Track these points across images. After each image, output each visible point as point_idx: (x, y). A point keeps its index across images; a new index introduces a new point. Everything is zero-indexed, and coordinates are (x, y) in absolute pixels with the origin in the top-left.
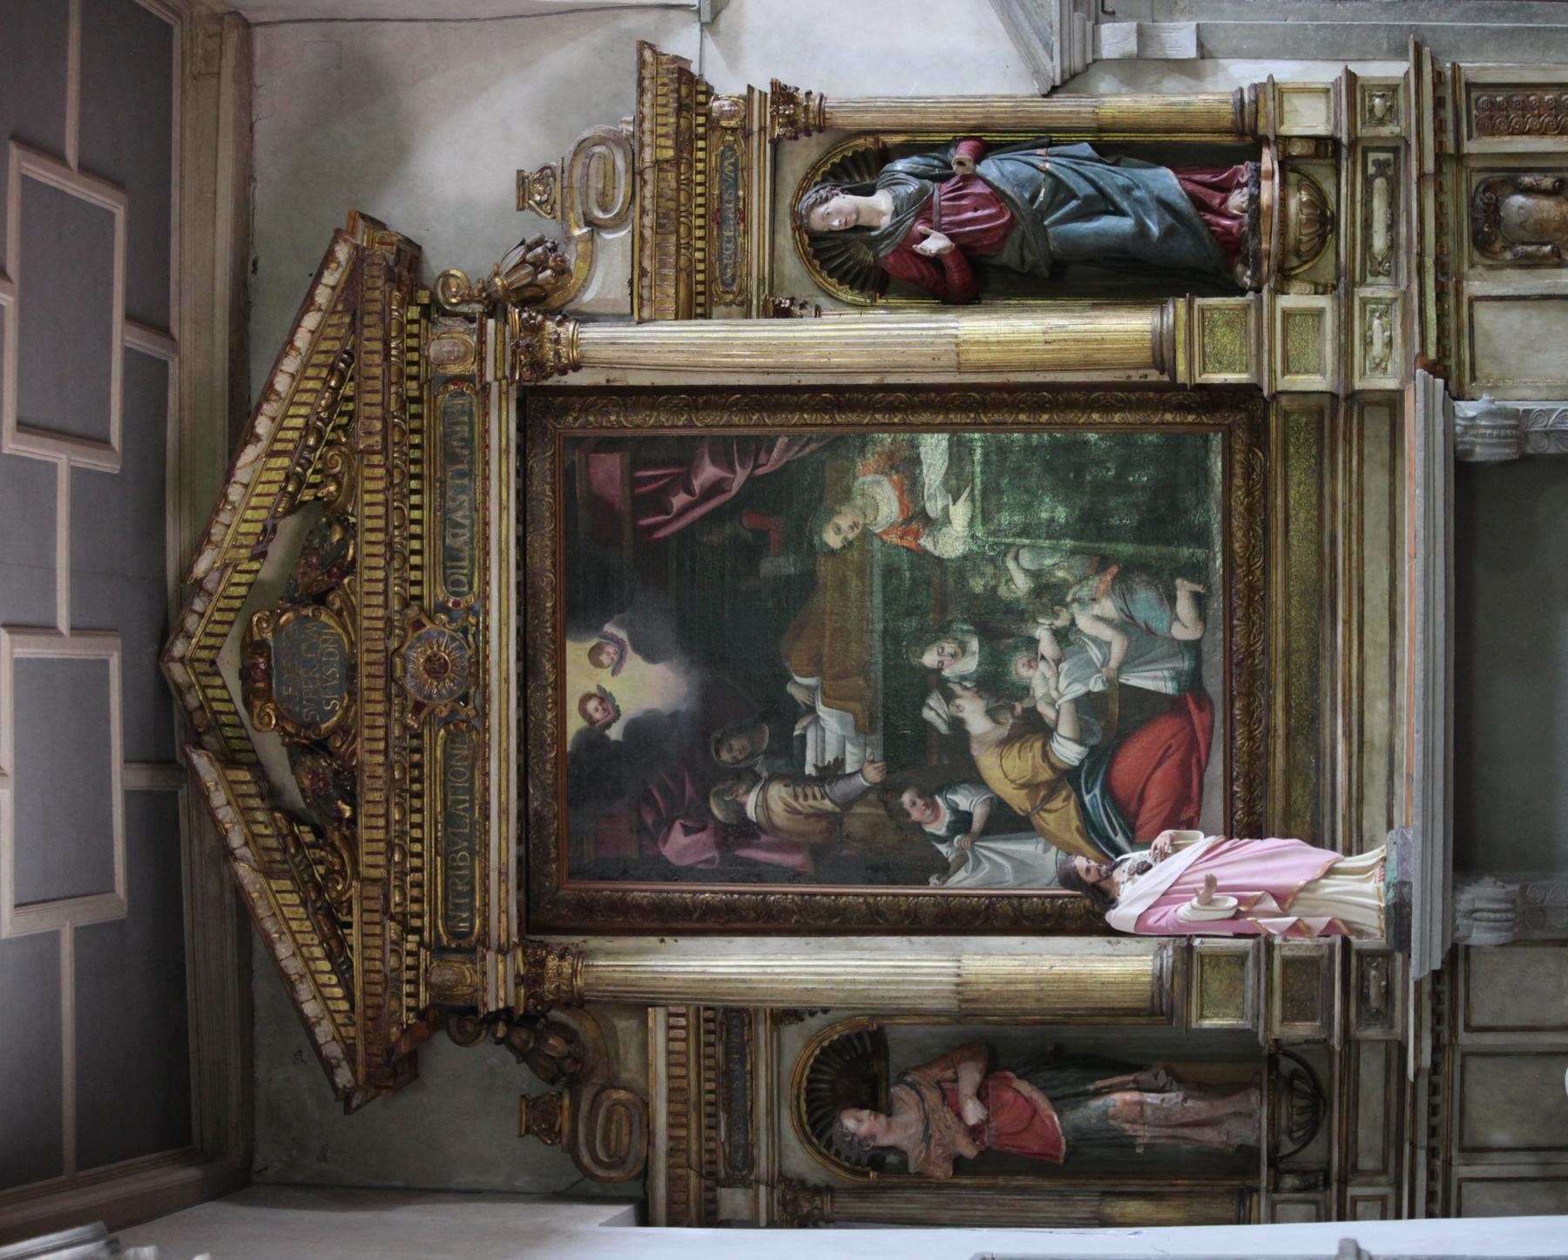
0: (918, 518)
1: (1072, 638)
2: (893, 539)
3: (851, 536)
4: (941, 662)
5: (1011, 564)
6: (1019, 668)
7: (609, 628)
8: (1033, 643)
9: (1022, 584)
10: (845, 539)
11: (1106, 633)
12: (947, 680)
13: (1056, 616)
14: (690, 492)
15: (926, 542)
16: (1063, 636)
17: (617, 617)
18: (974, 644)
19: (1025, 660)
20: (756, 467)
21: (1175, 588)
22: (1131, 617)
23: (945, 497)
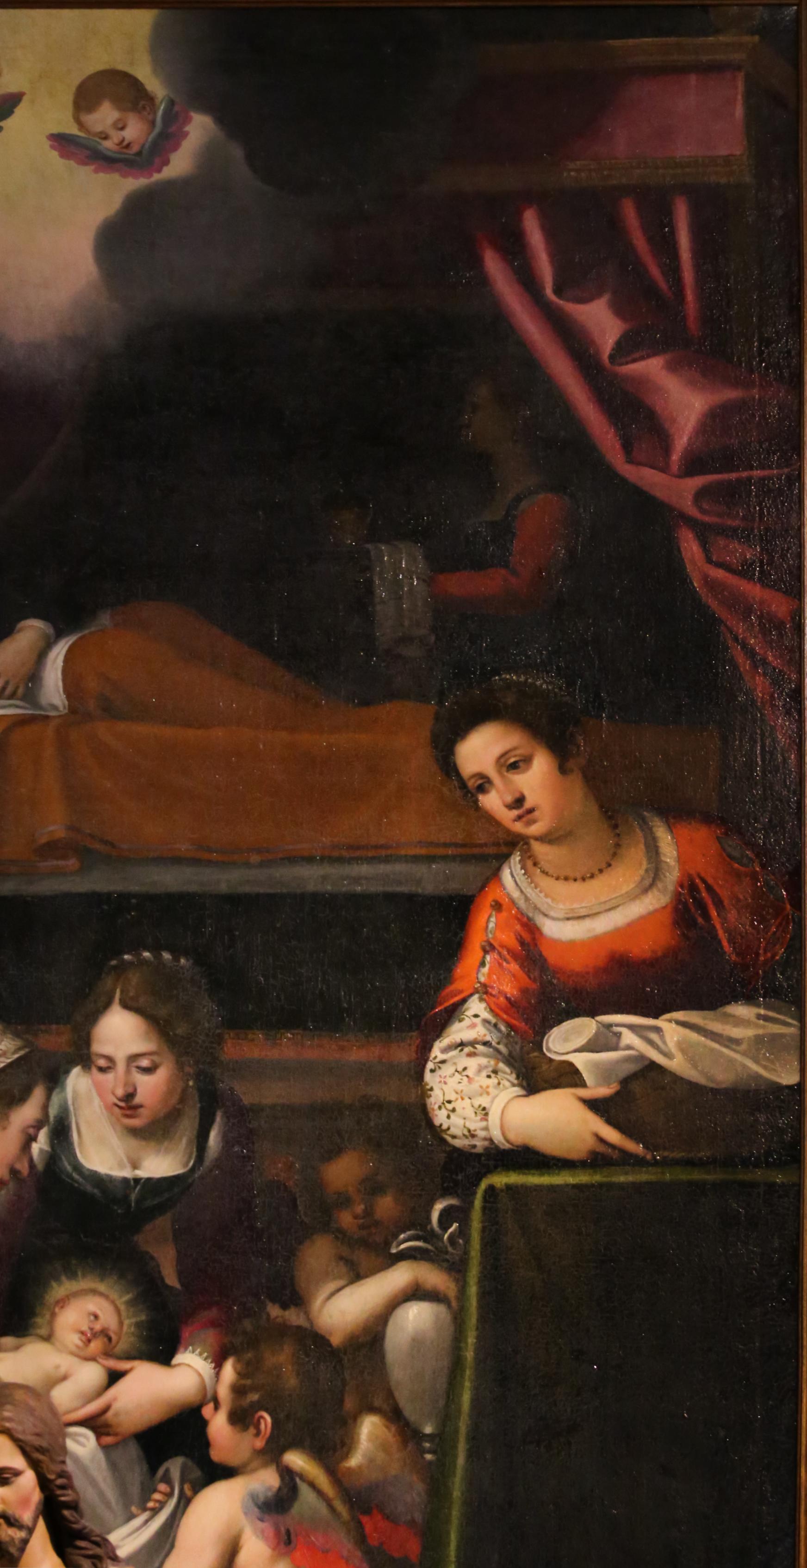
0: (549, 994)
1: (175, 1466)
2: (487, 925)
3: (493, 802)
4: (110, 1065)
5: (399, 1277)
6: (86, 1308)
7: (200, 128)
8: (161, 1349)
9: (343, 1308)
10: (484, 784)
12: (54, 1079)
13: (240, 1418)
14: (626, 348)
15: (474, 1022)
16: (173, 1447)
17: (237, 152)
18: (161, 1164)
19: (108, 1318)
20: (704, 533)
23: (604, 1073)
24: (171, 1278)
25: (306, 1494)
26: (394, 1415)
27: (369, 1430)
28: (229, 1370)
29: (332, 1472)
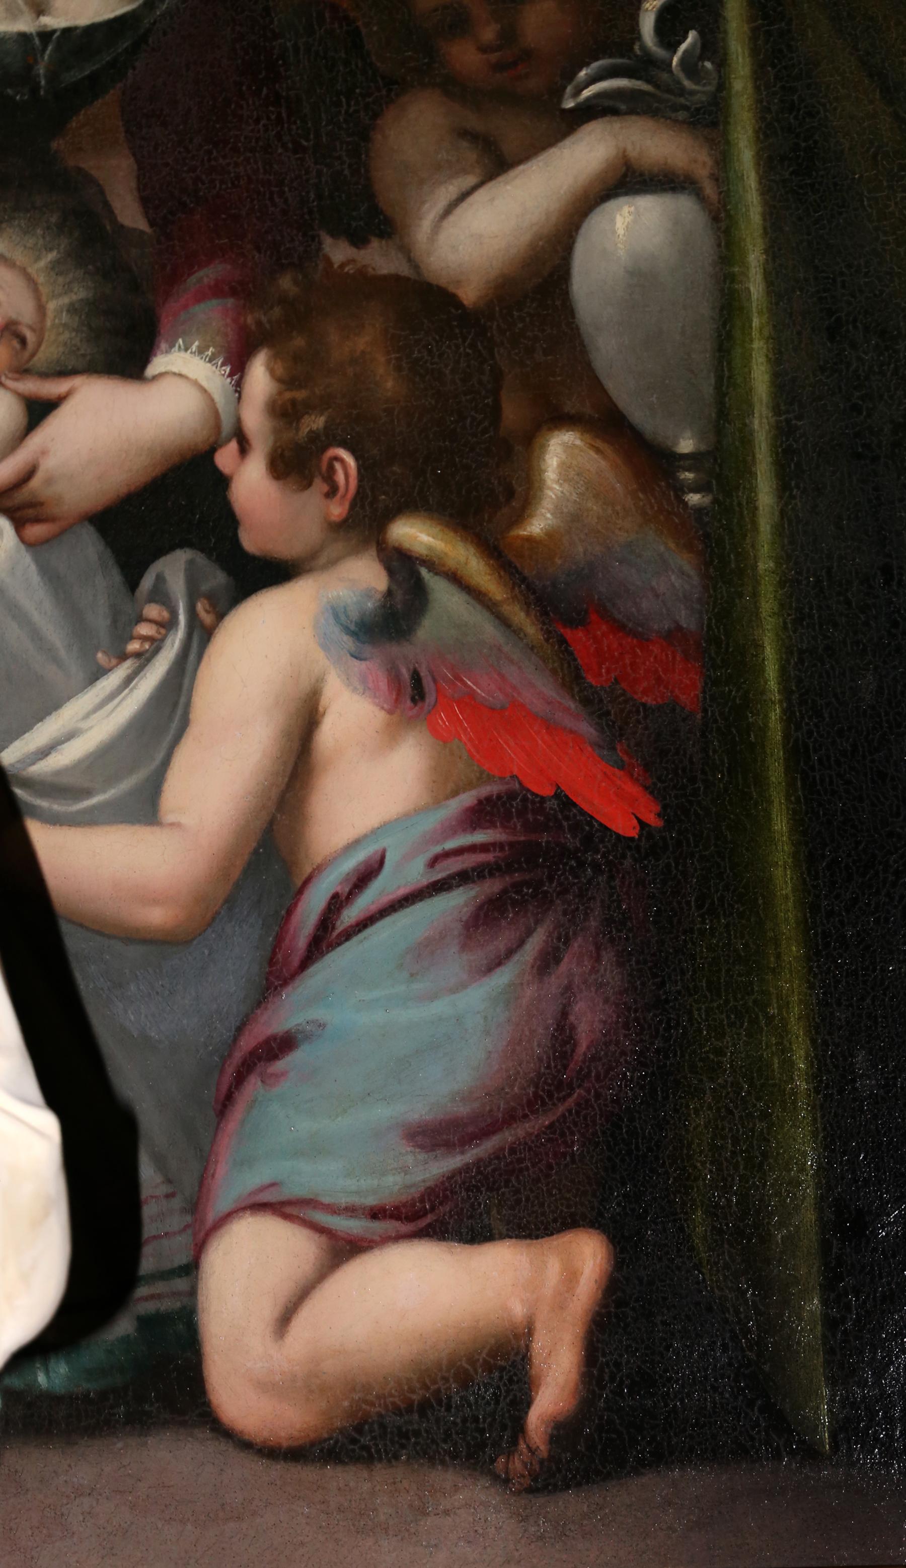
5: (586, 154)
8: (126, 353)
11: (215, 782)
13: (294, 464)
21: (532, 1224)
22: (326, 937)
24: (129, 213)
25: (444, 597)
26: (609, 424)
27: (562, 461)
28: (260, 376)
29: (495, 551)
